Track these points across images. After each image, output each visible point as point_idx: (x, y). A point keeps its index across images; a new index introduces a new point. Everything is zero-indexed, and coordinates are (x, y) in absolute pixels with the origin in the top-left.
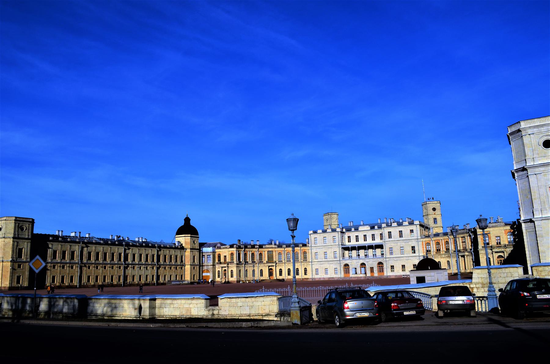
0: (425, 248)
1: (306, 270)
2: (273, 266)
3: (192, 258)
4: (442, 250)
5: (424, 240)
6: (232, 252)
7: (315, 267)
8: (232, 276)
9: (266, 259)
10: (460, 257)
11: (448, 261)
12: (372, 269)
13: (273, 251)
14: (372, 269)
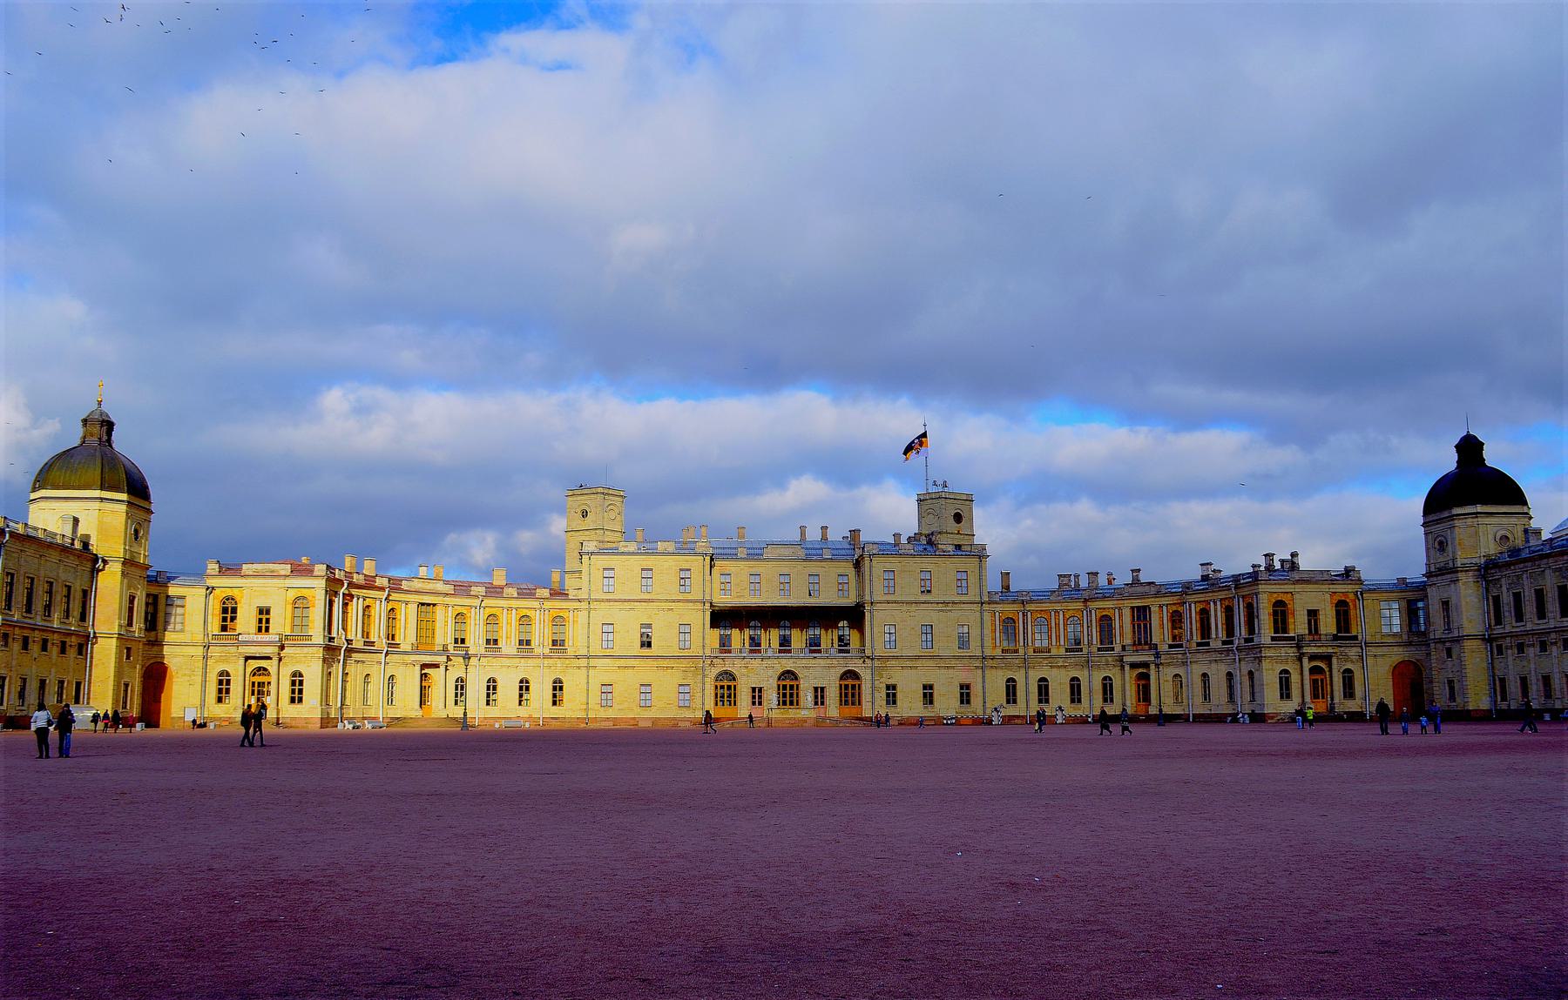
0: (998, 634)
1: (558, 686)
2: (436, 666)
3: (126, 604)
4: (1054, 643)
5: (999, 608)
6: (305, 593)
7: (597, 678)
8: (297, 697)
9: (412, 638)
10: (1127, 668)
12: (819, 694)
13: (434, 605)
14: (819, 694)
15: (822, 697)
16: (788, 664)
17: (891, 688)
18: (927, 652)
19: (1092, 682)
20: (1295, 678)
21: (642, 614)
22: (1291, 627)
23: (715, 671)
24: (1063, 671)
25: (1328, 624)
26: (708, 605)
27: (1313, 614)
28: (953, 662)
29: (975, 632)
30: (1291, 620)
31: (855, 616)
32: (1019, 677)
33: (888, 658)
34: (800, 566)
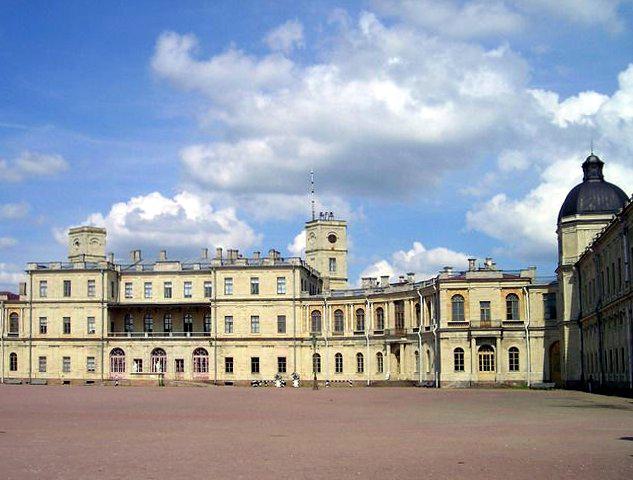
7: (38, 352)
11: (359, 354)
12: (180, 363)
14: (180, 363)
15: (182, 366)
16: (159, 344)
17: (229, 361)
18: (255, 336)
19: (370, 355)
20: (467, 354)
21: (65, 311)
22: (466, 315)
23: (110, 349)
24: (351, 348)
25: (499, 313)
26: (105, 305)
27: (485, 304)
28: (273, 343)
29: (289, 321)
30: (466, 310)
31: (202, 311)
32: (321, 352)
33: (226, 340)
34: (178, 277)
